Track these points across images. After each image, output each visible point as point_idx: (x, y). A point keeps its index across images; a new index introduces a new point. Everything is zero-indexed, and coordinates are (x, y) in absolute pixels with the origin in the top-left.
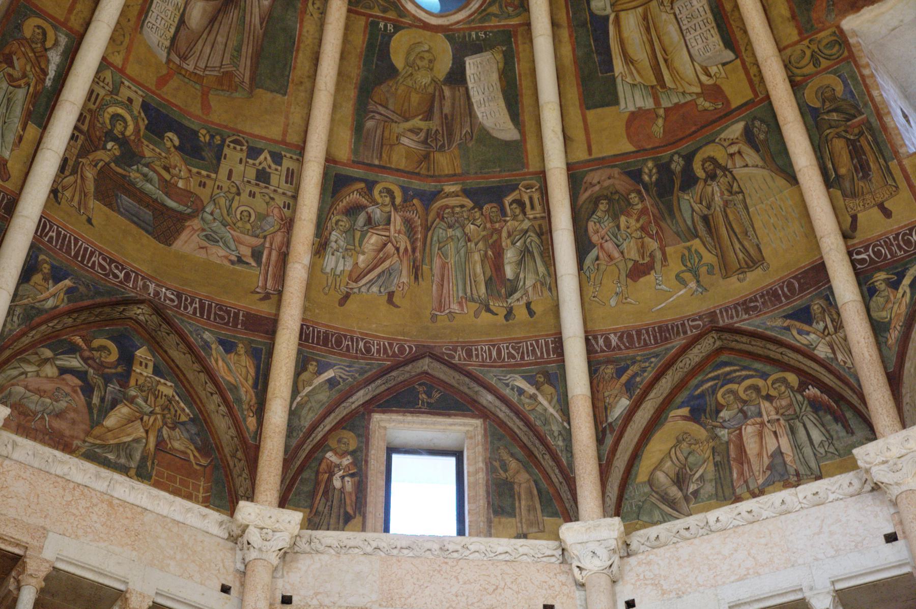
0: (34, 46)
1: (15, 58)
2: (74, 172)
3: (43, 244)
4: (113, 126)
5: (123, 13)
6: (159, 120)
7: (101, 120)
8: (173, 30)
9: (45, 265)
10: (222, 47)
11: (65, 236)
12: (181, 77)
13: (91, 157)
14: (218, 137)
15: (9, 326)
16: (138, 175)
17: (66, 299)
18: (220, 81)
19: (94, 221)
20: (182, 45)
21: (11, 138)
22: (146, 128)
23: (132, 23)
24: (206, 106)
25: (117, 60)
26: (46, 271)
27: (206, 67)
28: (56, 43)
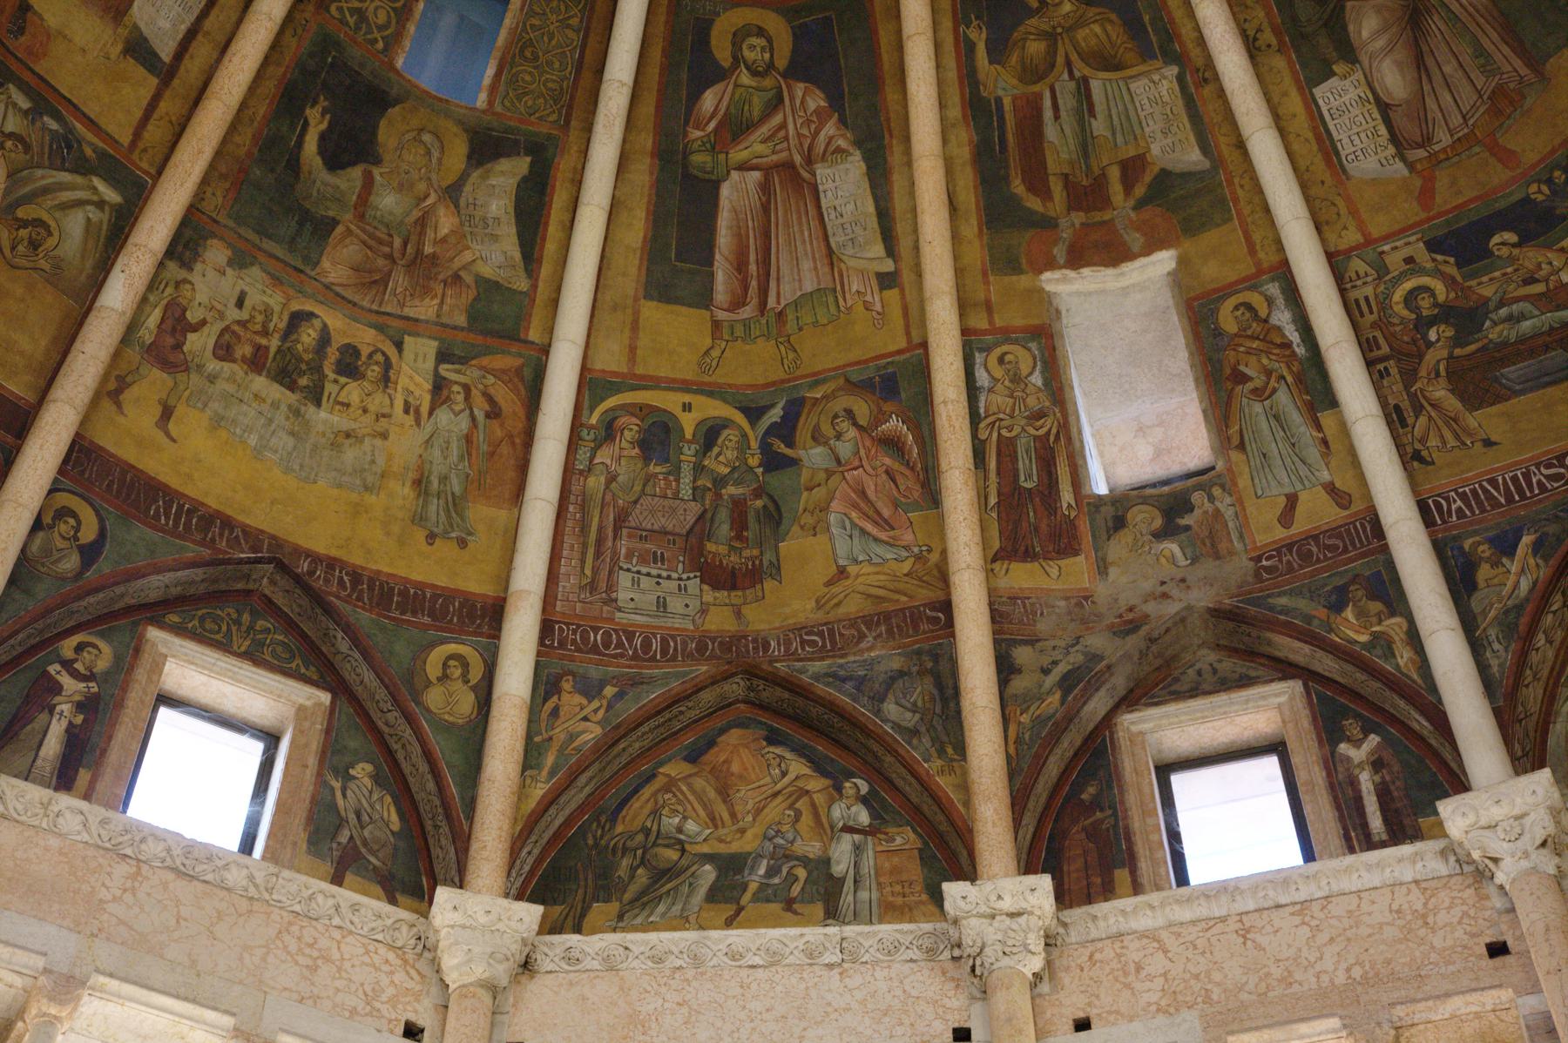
0: (1249, 333)
1: (1242, 368)
2: (1418, 409)
3: (1455, 527)
4: (1416, 309)
5: (1304, 187)
6: (1463, 243)
7: (1395, 321)
8: (1383, 130)
9: (1481, 548)
10: (1460, 72)
11: (1474, 492)
12: (1443, 165)
13: (1423, 373)
14: (1557, 173)
15: (1494, 663)
16: (1498, 329)
17: (1540, 562)
18: (1495, 112)
19: (1494, 438)
20: (1409, 129)
21: (1313, 454)
22: (1459, 265)
23: (1329, 180)
24: (1506, 157)
25: (1352, 237)
26: (1487, 554)
27: (1464, 117)
28: (1270, 302)
